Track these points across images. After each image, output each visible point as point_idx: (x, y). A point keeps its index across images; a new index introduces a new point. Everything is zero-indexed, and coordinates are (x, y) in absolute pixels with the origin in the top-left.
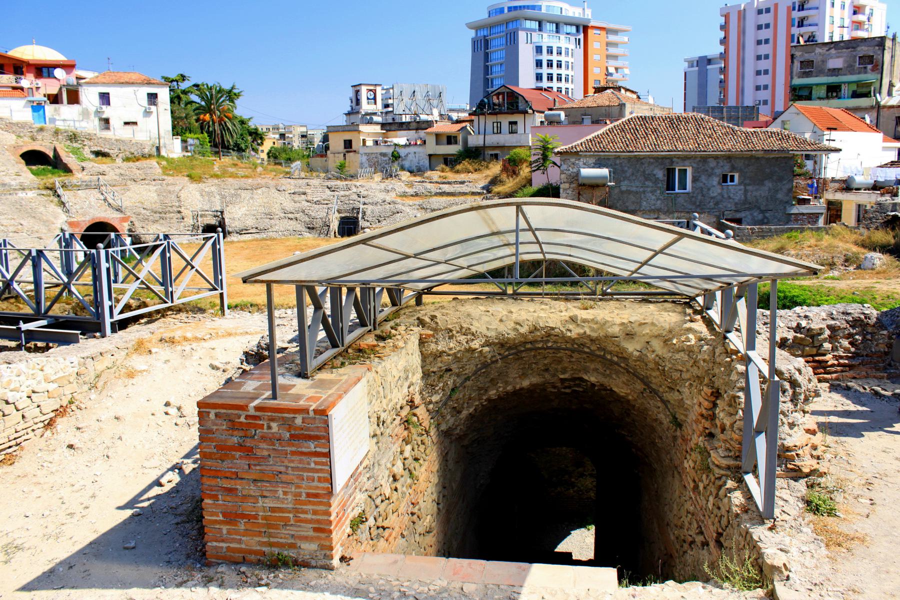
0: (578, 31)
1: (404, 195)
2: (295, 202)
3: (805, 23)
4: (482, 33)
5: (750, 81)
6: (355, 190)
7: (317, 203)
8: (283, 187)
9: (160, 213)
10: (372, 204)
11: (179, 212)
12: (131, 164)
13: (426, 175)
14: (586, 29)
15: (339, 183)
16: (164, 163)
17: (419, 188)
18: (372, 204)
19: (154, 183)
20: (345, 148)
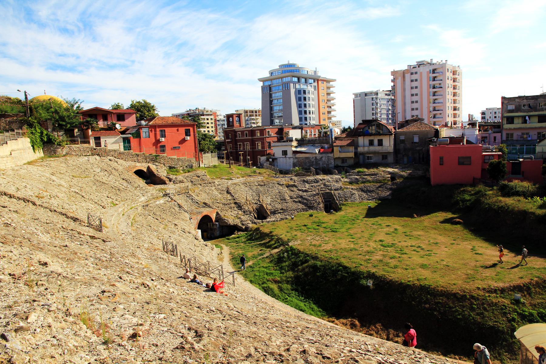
0: (314, 82)
3: (436, 79)
4: (267, 83)
5: (409, 106)
10: (336, 190)
11: (235, 203)
14: (318, 80)
18: (336, 190)
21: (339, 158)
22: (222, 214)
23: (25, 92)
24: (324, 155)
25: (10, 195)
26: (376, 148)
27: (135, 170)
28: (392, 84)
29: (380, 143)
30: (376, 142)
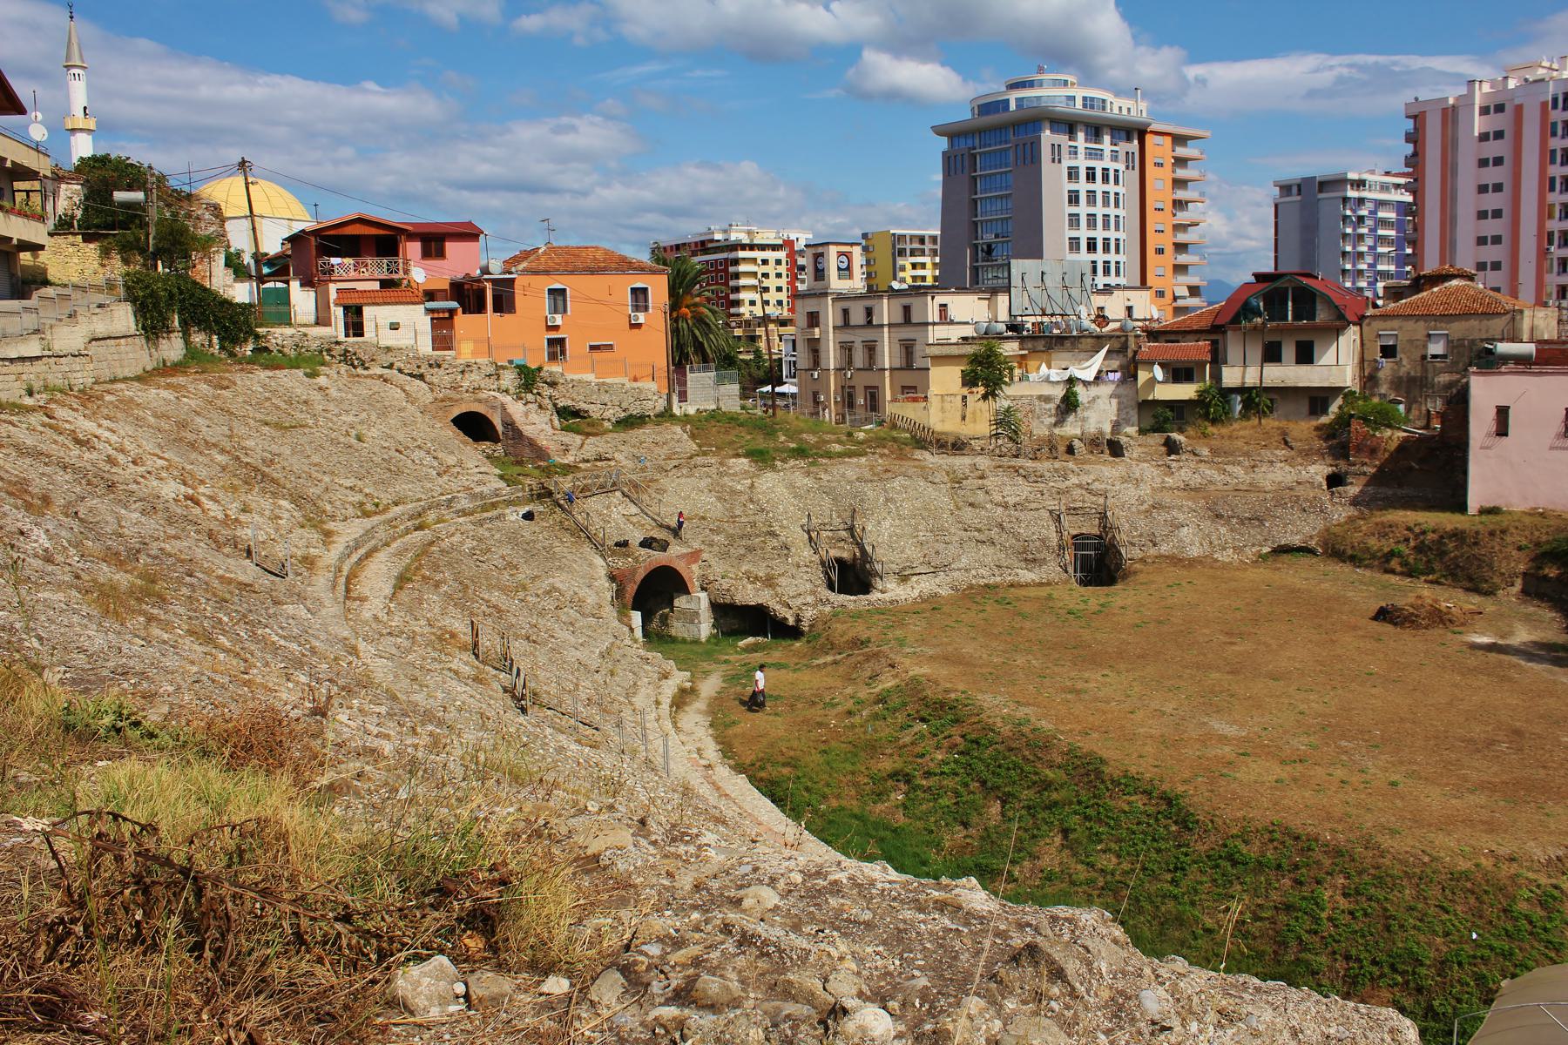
5: (1467, 228)
26: (1286, 373)
27: (456, 412)
28: (1409, 149)
29: (1305, 355)
30: (1289, 352)
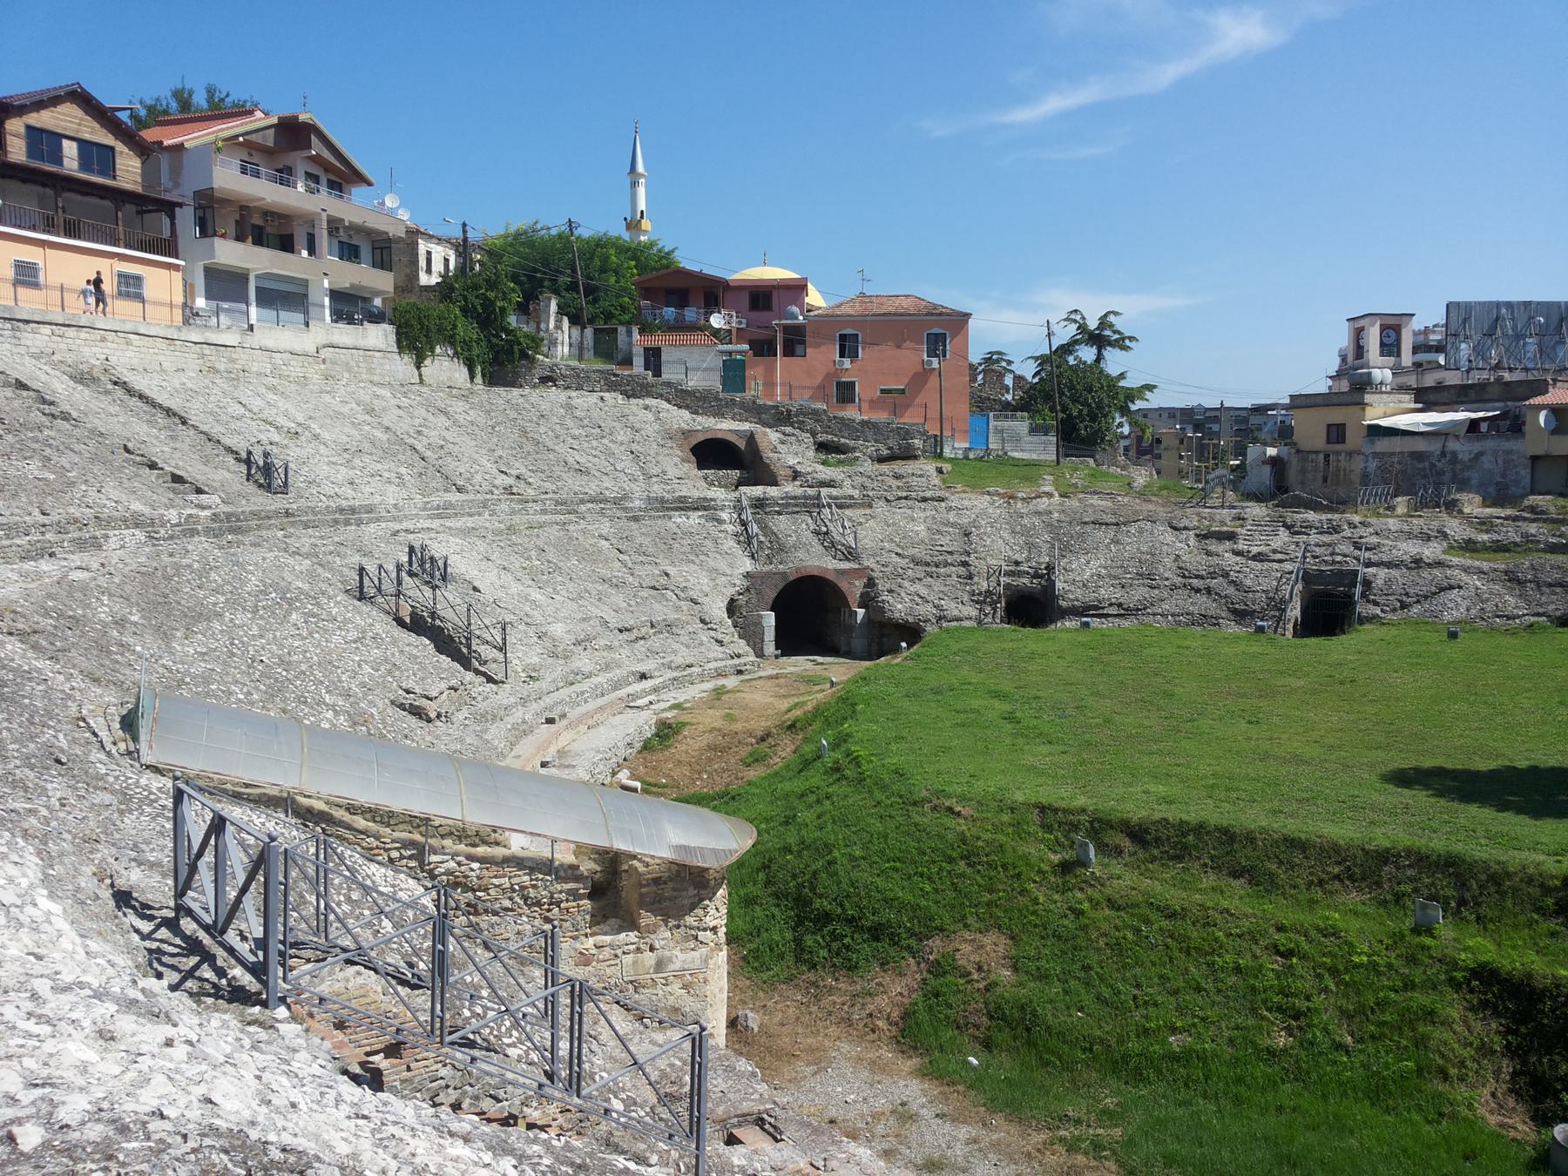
1: (1469, 547)
2: (1208, 553)
6: (1348, 533)
7: (1259, 557)
8: (1185, 522)
9: (928, 564)
10: (1389, 565)
12: (885, 468)
13: (1527, 502)
15: (1311, 516)
16: (947, 467)
17: (1511, 534)
18: (1389, 565)
19: (923, 505)
20: (1328, 442)
21: (1548, 457)
22: (882, 585)
23: (464, 225)
24: (1490, 444)
25: (147, 398)
